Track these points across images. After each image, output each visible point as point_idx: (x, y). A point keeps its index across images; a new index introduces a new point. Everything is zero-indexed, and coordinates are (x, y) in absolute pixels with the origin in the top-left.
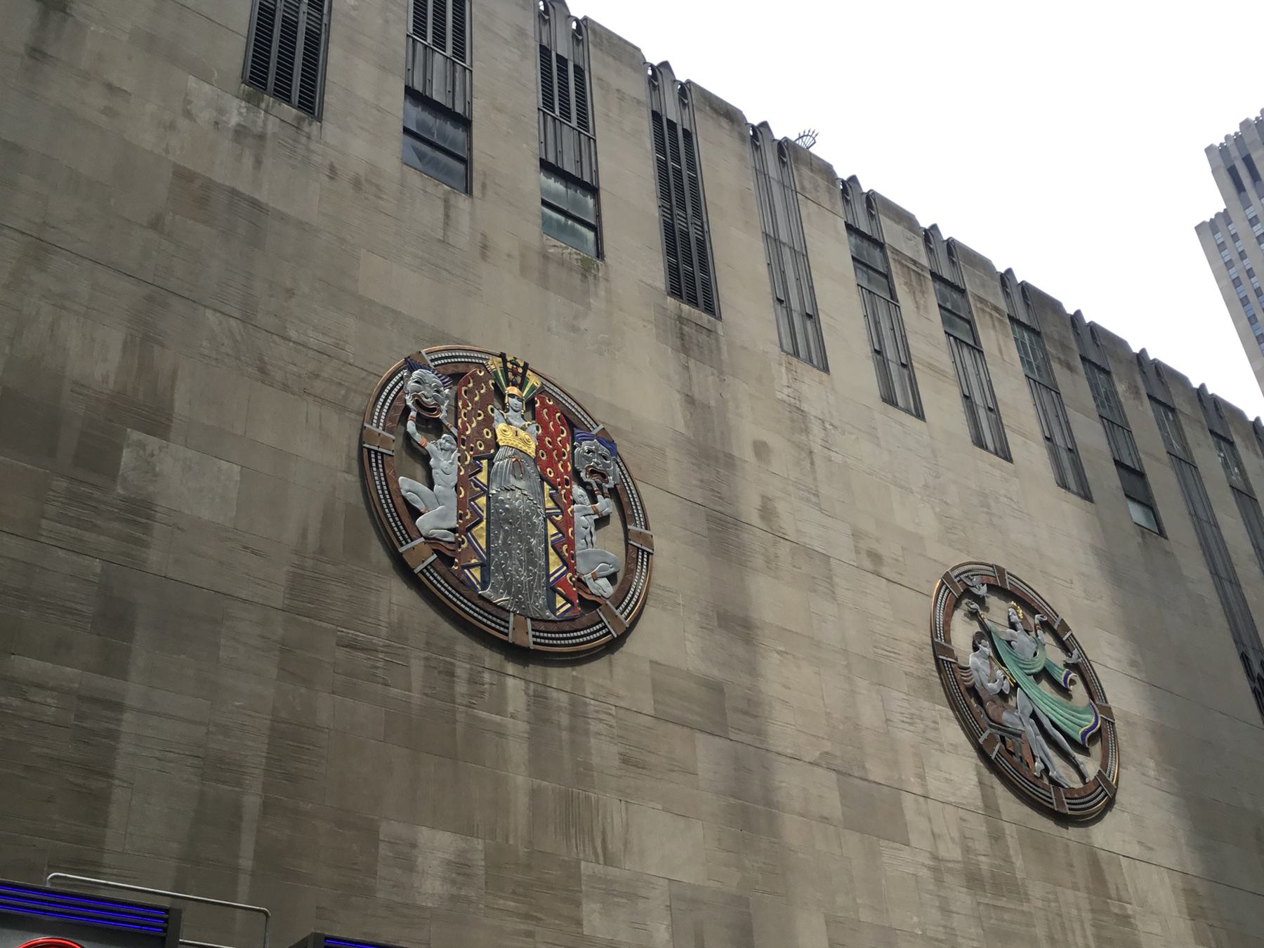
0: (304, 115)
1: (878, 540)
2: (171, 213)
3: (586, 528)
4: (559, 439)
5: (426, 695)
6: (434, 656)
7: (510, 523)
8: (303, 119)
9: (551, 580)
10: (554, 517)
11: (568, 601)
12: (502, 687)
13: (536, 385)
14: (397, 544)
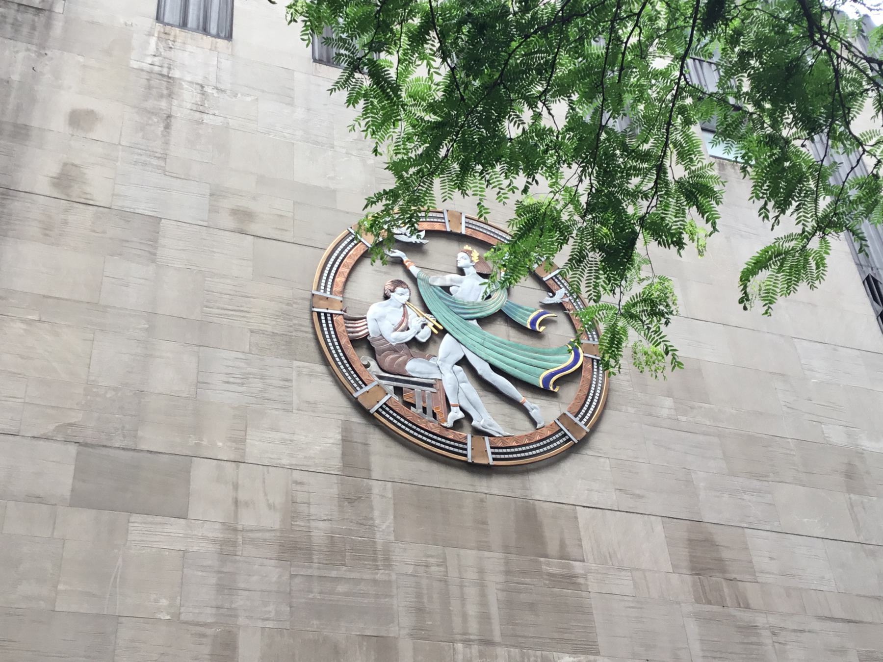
1: (254, 198)
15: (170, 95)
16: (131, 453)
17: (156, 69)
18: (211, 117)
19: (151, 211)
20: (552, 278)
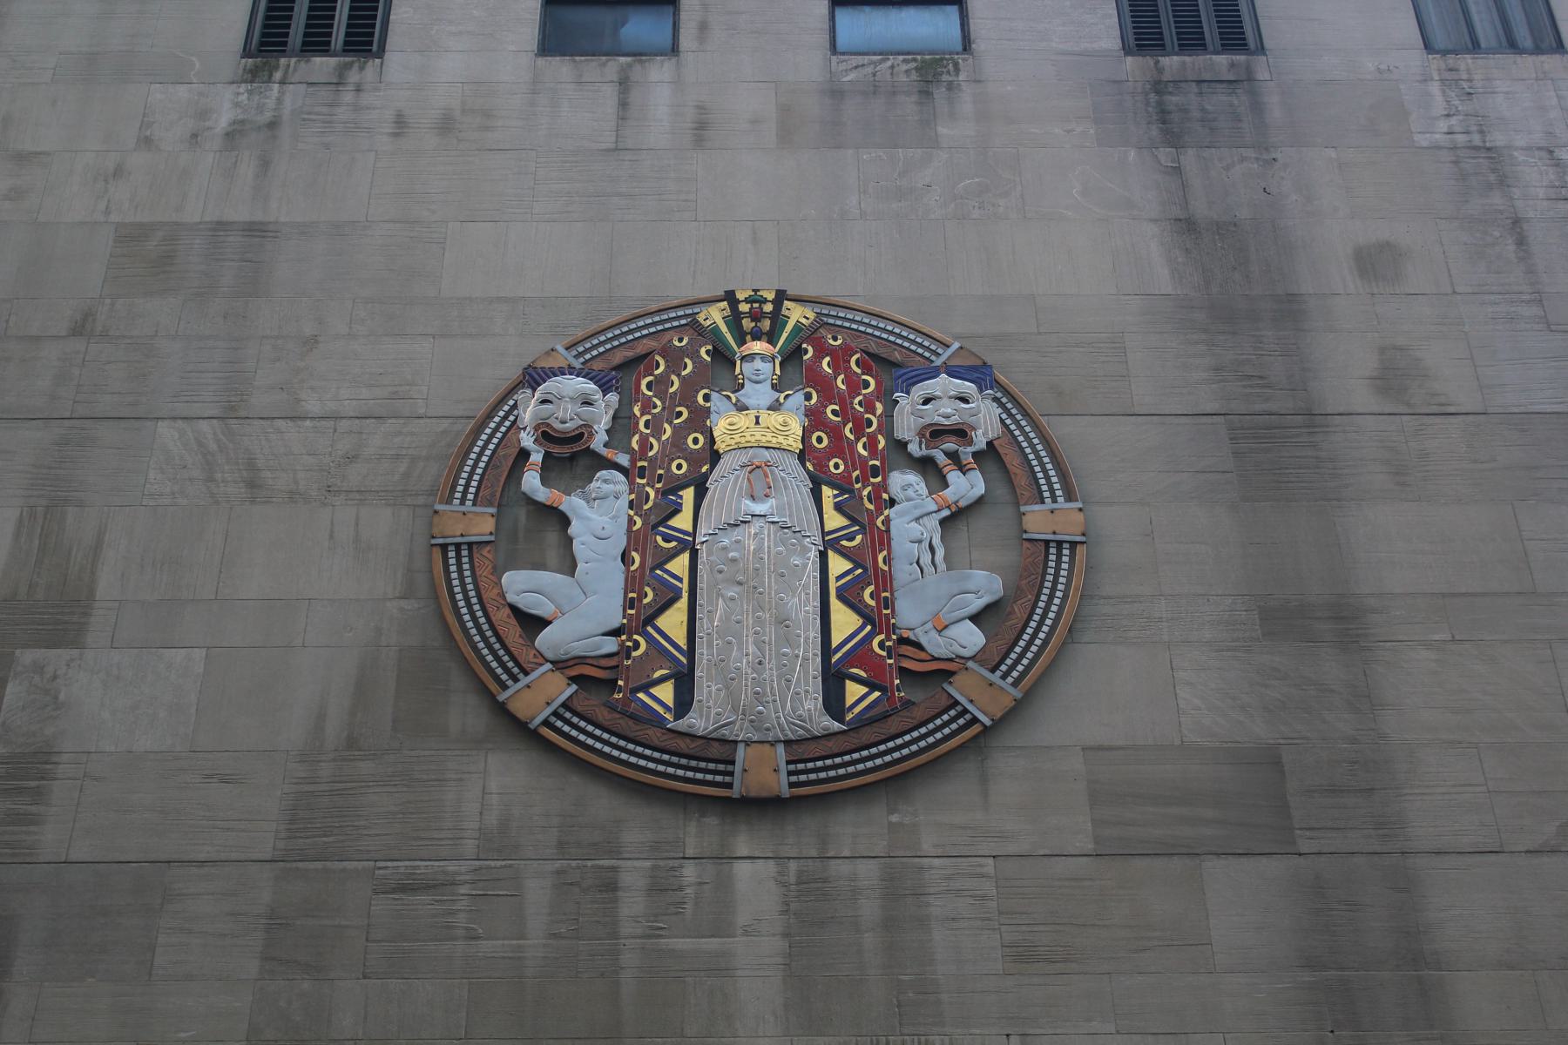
0: (350, 59)
2: (108, 301)
3: (920, 542)
4: (857, 400)
5: (555, 936)
6: (574, 863)
7: (740, 583)
8: (348, 66)
9: (833, 661)
10: (844, 543)
11: (872, 687)
12: (724, 885)
13: (804, 321)
14: (493, 687)
19: (1557, 403)
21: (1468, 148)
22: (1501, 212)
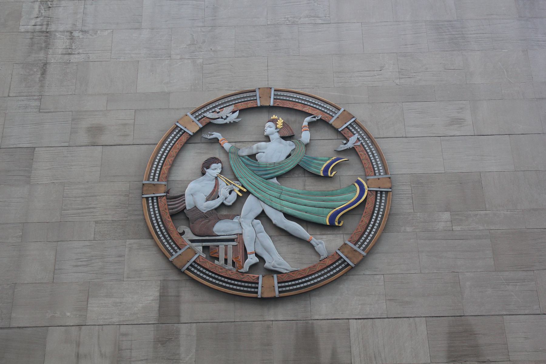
15: (47, 47)
16: (6, 331)
17: (38, 28)
18: (76, 56)
19: (28, 143)
20: (347, 127)
21: (40, 32)
22: (41, 60)
